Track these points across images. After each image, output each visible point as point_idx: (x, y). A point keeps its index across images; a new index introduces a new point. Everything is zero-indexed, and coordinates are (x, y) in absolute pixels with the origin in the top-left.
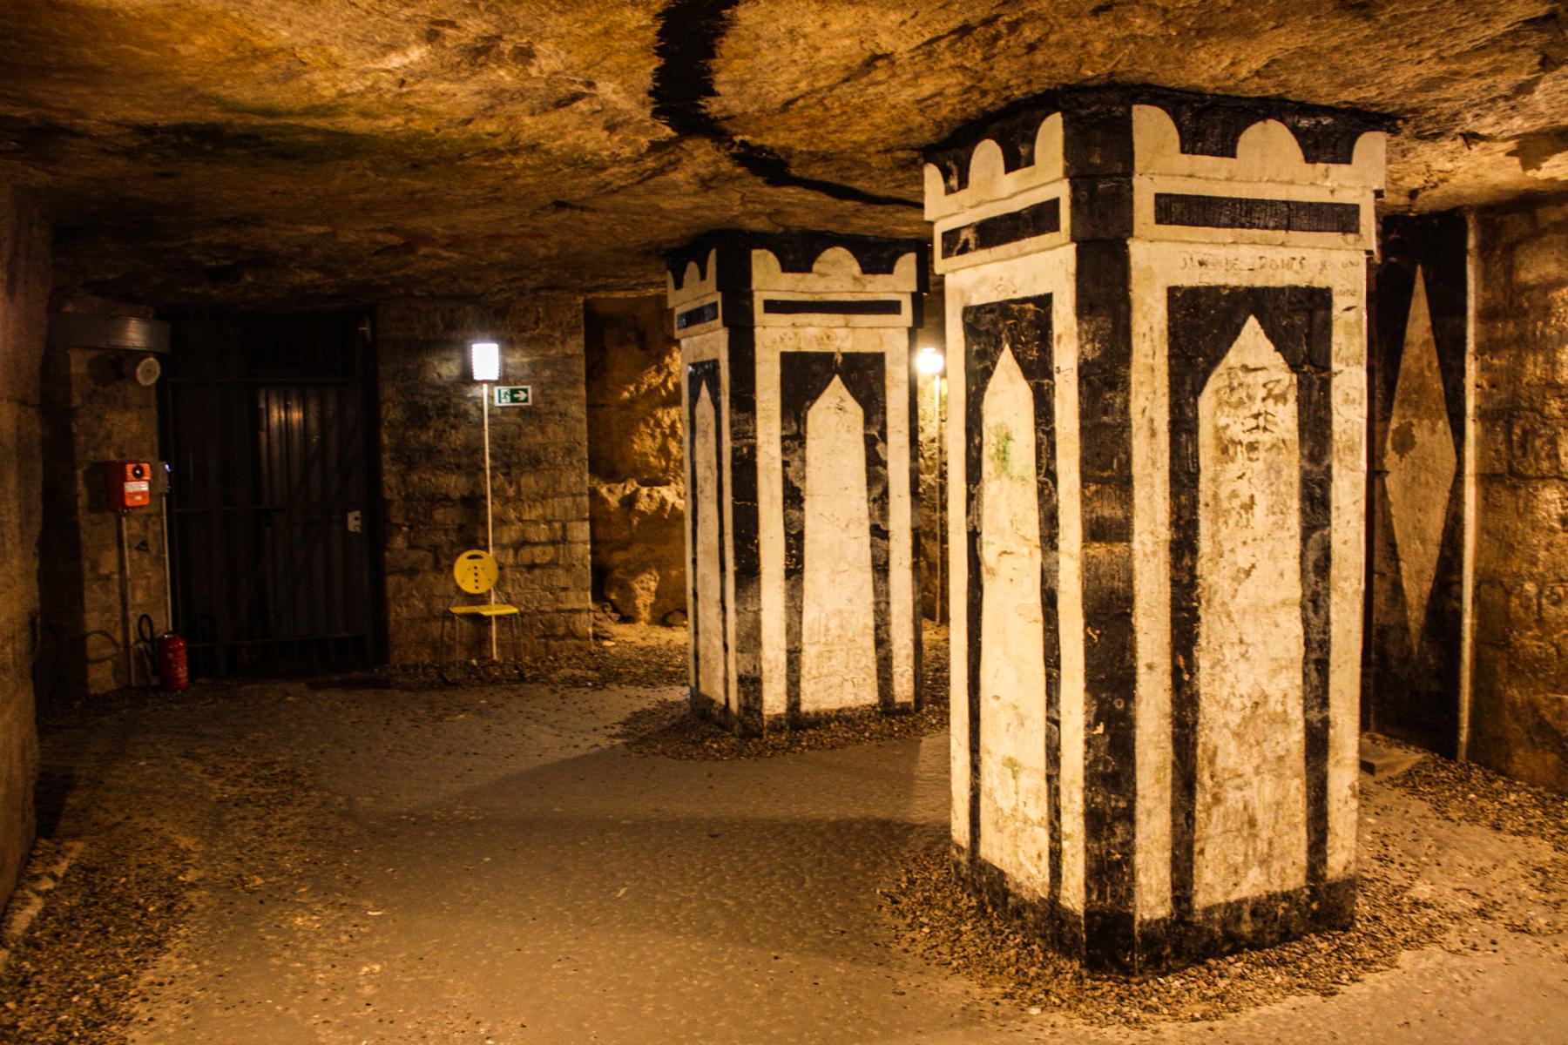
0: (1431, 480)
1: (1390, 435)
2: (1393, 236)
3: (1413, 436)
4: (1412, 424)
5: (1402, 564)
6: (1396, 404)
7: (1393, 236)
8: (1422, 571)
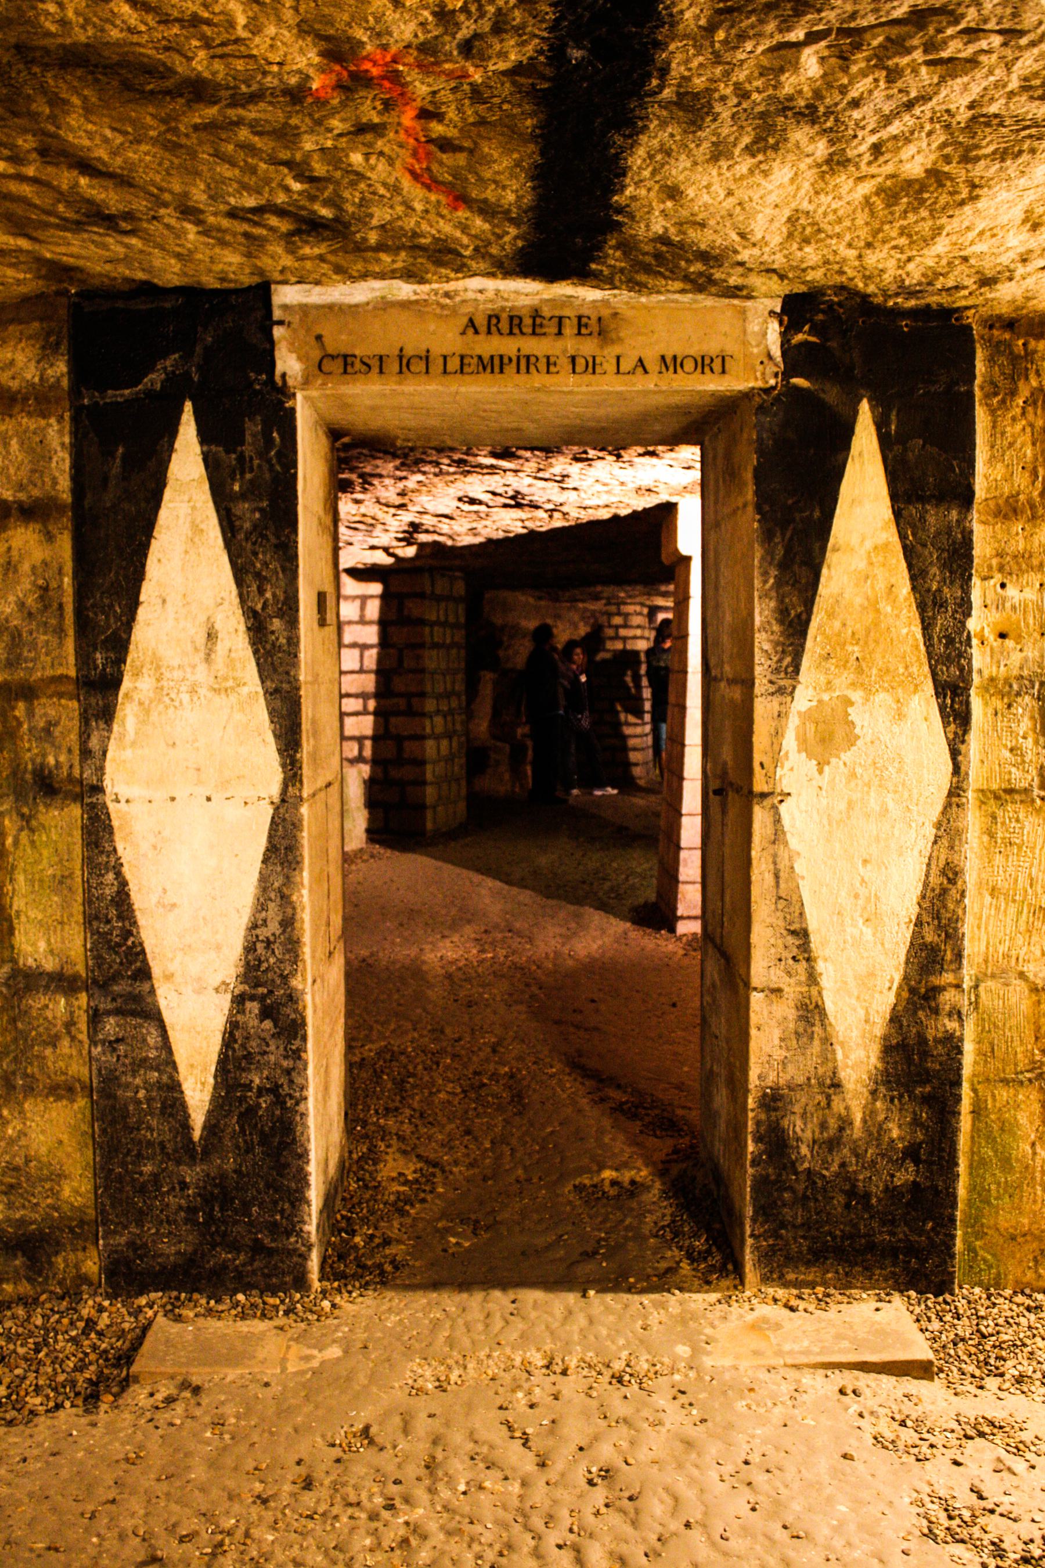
0: (891, 805)
1: (793, 723)
2: (800, 337)
4: (850, 703)
5: (820, 966)
6: (806, 662)
7: (800, 337)
8: (872, 975)
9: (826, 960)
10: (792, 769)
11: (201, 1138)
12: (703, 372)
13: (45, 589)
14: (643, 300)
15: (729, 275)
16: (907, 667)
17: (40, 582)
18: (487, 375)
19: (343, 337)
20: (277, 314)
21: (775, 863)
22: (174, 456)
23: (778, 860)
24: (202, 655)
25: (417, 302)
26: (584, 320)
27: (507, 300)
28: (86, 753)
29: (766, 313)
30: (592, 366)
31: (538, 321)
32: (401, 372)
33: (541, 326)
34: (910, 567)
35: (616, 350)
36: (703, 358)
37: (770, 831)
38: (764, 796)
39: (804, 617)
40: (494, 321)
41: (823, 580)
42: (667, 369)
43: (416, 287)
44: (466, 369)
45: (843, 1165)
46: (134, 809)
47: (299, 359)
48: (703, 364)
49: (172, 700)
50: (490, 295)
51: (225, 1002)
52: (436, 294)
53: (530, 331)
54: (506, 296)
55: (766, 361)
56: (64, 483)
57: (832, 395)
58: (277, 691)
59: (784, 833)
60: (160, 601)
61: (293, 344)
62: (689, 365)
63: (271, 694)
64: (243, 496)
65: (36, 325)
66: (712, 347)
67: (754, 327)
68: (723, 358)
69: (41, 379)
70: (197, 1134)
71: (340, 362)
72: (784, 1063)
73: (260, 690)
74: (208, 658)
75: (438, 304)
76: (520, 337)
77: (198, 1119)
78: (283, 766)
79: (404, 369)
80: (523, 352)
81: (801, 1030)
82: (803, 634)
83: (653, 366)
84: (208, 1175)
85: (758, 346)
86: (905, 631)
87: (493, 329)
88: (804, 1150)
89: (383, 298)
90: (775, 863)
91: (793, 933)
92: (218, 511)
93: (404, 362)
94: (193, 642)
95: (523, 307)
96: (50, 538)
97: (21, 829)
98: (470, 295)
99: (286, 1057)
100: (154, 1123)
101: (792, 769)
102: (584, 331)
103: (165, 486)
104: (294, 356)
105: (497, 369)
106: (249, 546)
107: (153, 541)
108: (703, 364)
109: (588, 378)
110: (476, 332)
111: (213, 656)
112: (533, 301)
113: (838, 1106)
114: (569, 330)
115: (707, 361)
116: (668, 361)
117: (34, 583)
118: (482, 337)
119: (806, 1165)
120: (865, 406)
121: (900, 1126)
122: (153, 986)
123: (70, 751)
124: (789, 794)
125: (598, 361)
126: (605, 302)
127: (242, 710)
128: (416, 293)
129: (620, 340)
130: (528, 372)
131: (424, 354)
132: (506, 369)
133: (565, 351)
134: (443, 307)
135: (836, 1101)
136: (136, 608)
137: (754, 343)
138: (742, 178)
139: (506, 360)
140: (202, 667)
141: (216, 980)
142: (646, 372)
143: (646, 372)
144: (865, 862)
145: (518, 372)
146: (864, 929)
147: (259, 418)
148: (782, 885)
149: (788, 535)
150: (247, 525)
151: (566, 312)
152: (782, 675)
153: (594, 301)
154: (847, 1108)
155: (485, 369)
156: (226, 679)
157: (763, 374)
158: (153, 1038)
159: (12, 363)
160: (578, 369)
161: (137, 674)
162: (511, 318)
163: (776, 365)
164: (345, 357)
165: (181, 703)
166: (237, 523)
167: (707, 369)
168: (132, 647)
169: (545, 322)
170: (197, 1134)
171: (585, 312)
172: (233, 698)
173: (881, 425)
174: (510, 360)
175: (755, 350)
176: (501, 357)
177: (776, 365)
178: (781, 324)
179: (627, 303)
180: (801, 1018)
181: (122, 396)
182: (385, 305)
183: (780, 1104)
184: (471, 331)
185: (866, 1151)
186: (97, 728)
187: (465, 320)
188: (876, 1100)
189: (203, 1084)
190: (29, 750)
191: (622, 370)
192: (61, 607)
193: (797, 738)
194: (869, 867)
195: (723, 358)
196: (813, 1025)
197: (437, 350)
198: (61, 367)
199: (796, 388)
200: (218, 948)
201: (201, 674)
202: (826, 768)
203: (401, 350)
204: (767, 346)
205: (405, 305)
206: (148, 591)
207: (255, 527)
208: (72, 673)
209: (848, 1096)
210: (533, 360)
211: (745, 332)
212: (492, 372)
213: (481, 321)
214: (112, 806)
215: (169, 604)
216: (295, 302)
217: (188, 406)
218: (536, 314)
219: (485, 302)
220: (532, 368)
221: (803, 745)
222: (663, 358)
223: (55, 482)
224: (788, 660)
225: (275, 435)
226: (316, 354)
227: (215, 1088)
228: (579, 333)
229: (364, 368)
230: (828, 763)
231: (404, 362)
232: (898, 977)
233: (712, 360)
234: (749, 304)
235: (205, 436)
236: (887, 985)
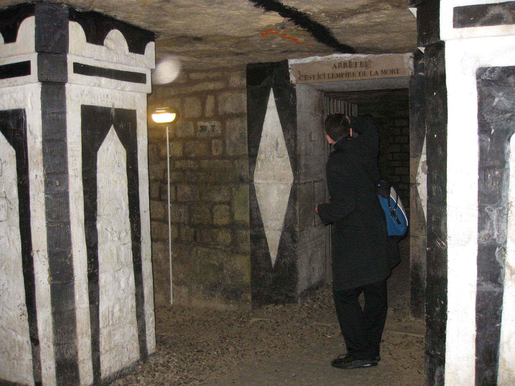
13: (241, 134)
17: (241, 132)
20: (289, 67)
22: (269, 101)
26: (362, 63)
27: (343, 59)
28: (250, 172)
31: (351, 64)
33: (351, 65)
35: (370, 69)
44: (333, 77)
46: (260, 186)
47: (295, 77)
49: (268, 159)
50: (339, 58)
52: (326, 59)
53: (349, 66)
56: (246, 108)
61: (293, 73)
62: (389, 72)
65: (239, 72)
66: (395, 67)
68: (398, 70)
69: (241, 84)
73: (288, 157)
74: (276, 150)
75: (327, 61)
78: (294, 175)
79: (319, 77)
80: (347, 72)
83: (379, 73)
89: (314, 61)
93: (319, 76)
94: (273, 145)
95: (347, 60)
96: (242, 121)
97: (236, 190)
98: (334, 58)
102: (362, 65)
104: (293, 76)
105: (341, 76)
108: (392, 72)
110: (336, 67)
112: (350, 59)
114: (358, 65)
115: (393, 71)
116: (384, 71)
117: (239, 132)
123: (247, 172)
125: (366, 72)
126: (367, 58)
127: (284, 162)
128: (321, 59)
131: (323, 74)
132: (343, 76)
134: (328, 62)
137: (405, 65)
139: (343, 74)
140: (275, 152)
141: (278, 228)
142: (378, 75)
143: (378, 75)
145: (346, 77)
155: (338, 77)
156: (281, 154)
159: (234, 81)
161: (261, 154)
162: (344, 64)
163: (412, 70)
164: (305, 76)
167: (393, 73)
168: (260, 147)
169: (353, 64)
171: (362, 60)
172: (282, 159)
175: (406, 67)
176: (342, 73)
177: (412, 70)
182: (313, 63)
184: (335, 67)
186: (252, 166)
187: (333, 65)
189: (275, 253)
190: (238, 171)
192: (245, 138)
195: (398, 70)
198: (244, 81)
199: (420, 75)
200: (278, 220)
201: (275, 153)
203: (318, 73)
204: (409, 66)
208: (247, 153)
210: (349, 74)
211: (403, 63)
213: (337, 65)
214: (255, 185)
215: (268, 137)
217: (272, 89)
218: (350, 62)
219: (338, 60)
220: (350, 76)
222: (382, 71)
223: (244, 108)
227: (277, 255)
228: (361, 66)
231: (319, 76)
233: (395, 70)
235: (275, 96)
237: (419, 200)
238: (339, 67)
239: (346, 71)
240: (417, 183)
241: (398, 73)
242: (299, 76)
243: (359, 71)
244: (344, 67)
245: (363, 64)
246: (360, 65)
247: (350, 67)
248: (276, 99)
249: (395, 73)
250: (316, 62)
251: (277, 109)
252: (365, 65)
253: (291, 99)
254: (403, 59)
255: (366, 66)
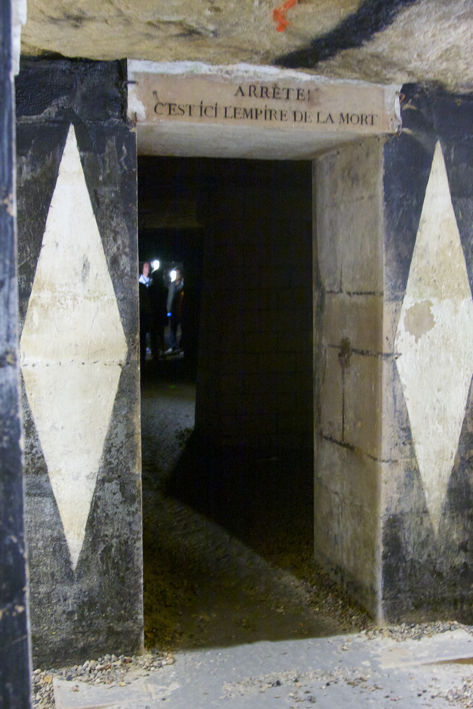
0: (451, 359)
1: (403, 315)
2: (407, 106)
3: (432, 316)
4: (430, 304)
5: (417, 447)
7: (407, 106)
8: (442, 451)
9: (419, 444)
10: (402, 340)
11: (77, 568)
12: (362, 123)
14: (332, 82)
15: (389, 73)
16: (459, 285)
18: (248, 120)
19: (169, 93)
20: (130, 77)
21: (394, 391)
22: (63, 158)
23: (396, 390)
24: (81, 277)
25: (210, 76)
26: (301, 92)
27: (260, 78)
29: (394, 93)
30: (305, 118)
31: (276, 91)
32: (201, 115)
33: (278, 93)
34: (460, 231)
35: (318, 109)
36: (362, 116)
37: (391, 374)
38: (388, 355)
39: (408, 257)
40: (253, 89)
41: (418, 238)
42: (344, 121)
43: (210, 67)
44: (237, 115)
45: (429, 556)
47: (144, 104)
48: (362, 119)
49: (62, 304)
50: (251, 74)
51: (93, 485)
52: (221, 72)
53: (272, 95)
54: (259, 75)
55: (394, 119)
57: (422, 138)
58: (124, 298)
59: (398, 375)
60: (54, 244)
62: (355, 119)
63: (121, 300)
64: (105, 183)
66: (367, 111)
67: (388, 100)
70: (74, 566)
71: (167, 107)
72: (399, 500)
73: (114, 298)
74: (84, 279)
75: (222, 77)
76: (266, 99)
77: (75, 557)
78: (128, 343)
80: (268, 108)
81: (407, 483)
82: (408, 267)
83: (336, 118)
84: (81, 590)
85: (390, 110)
86: (458, 266)
87: (252, 93)
88: (410, 549)
89: (192, 72)
90: (394, 391)
91: (403, 429)
92: (89, 192)
95: (269, 82)
98: (240, 73)
99: (129, 515)
100: (48, 562)
101: (402, 340)
102: (300, 97)
103: (57, 175)
106: (108, 213)
107: (50, 209)
108: (362, 119)
109: (303, 124)
110: (243, 95)
111: (87, 278)
113: (426, 524)
114: (293, 95)
115: (364, 117)
116: (344, 116)
118: (247, 98)
119: (410, 557)
120: (438, 145)
121: (457, 532)
122: (48, 477)
124: (401, 354)
125: (308, 115)
126: (312, 82)
128: (210, 70)
129: (319, 104)
130: (271, 118)
131: (214, 106)
133: (291, 108)
134: (225, 79)
135: (425, 519)
136: (40, 249)
138: (444, 29)
139: (259, 112)
142: (332, 122)
143: (332, 122)
144: (439, 390)
146: (438, 426)
147: (114, 138)
148: (398, 404)
149: (400, 214)
150: (107, 201)
151: (291, 87)
152: (397, 289)
153: (306, 81)
154: (431, 524)
155: (247, 116)
157: (392, 126)
158: (48, 509)
160: (297, 119)
161: (41, 289)
162: (262, 89)
164: (170, 105)
165: (67, 305)
166: (101, 199)
170: (74, 566)
171: (302, 87)
173: (446, 156)
174: (261, 112)
175: (389, 113)
178: (400, 98)
179: (324, 83)
180: (407, 476)
181: (30, 120)
183: (397, 524)
184: (240, 94)
185: (441, 547)
187: (238, 88)
188: (445, 519)
189: (79, 535)
191: (320, 120)
193: (405, 324)
194: (440, 393)
196: (413, 479)
197: (221, 105)
201: (80, 289)
202: (420, 340)
203: (202, 103)
205: (204, 77)
206: (47, 238)
207: (112, 202)
209: (431, 517)
210: (273, 112)
212: (252, 117)
213: (246, 90)
216: (141, 71)
217: (72, 128)
218: (275, 87)
220: (273, 117)
221: (408, 328)
222: (341, 115)
224: (400, 281)
225: (124, 148)
226: (154, 103)
227: (86, 537)
228: (298, 98)
229: (180, 112)
230: (420, 337)
232: (455, 451)
233: (367, 118)
234: (386, 87)
235: (82, 146)
236: (450, 456)
237: (399, 387)
238: (250, 95)
239: (266, 106)
240: (395, 352)
241: (372, 123)
242: (155, 105)
243: (294, 109)
244: (262, 96)
245: (302, 95)
246: (297, 98)
247: (274, 97)
248: (82, 154)
249: (366, 122)
250: (197, 76)
251: (86, 178)
252: (307, 97)
253: (122, 159)
254: (383, 96)
255: (309, 100)
